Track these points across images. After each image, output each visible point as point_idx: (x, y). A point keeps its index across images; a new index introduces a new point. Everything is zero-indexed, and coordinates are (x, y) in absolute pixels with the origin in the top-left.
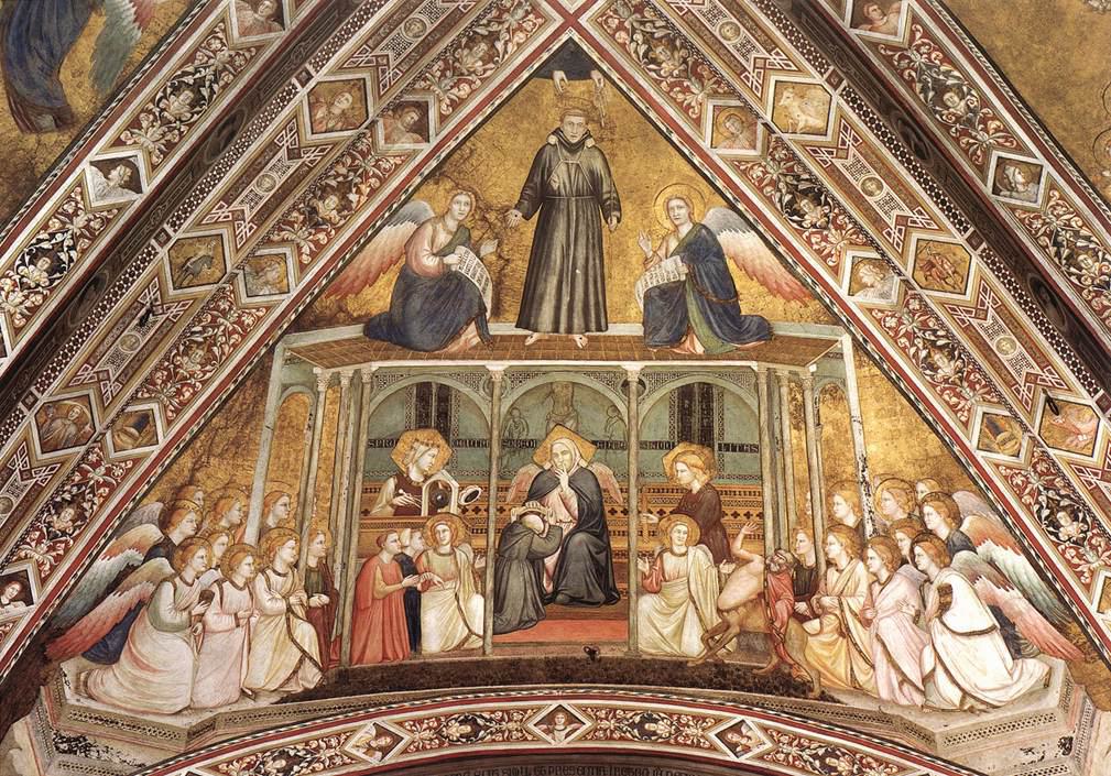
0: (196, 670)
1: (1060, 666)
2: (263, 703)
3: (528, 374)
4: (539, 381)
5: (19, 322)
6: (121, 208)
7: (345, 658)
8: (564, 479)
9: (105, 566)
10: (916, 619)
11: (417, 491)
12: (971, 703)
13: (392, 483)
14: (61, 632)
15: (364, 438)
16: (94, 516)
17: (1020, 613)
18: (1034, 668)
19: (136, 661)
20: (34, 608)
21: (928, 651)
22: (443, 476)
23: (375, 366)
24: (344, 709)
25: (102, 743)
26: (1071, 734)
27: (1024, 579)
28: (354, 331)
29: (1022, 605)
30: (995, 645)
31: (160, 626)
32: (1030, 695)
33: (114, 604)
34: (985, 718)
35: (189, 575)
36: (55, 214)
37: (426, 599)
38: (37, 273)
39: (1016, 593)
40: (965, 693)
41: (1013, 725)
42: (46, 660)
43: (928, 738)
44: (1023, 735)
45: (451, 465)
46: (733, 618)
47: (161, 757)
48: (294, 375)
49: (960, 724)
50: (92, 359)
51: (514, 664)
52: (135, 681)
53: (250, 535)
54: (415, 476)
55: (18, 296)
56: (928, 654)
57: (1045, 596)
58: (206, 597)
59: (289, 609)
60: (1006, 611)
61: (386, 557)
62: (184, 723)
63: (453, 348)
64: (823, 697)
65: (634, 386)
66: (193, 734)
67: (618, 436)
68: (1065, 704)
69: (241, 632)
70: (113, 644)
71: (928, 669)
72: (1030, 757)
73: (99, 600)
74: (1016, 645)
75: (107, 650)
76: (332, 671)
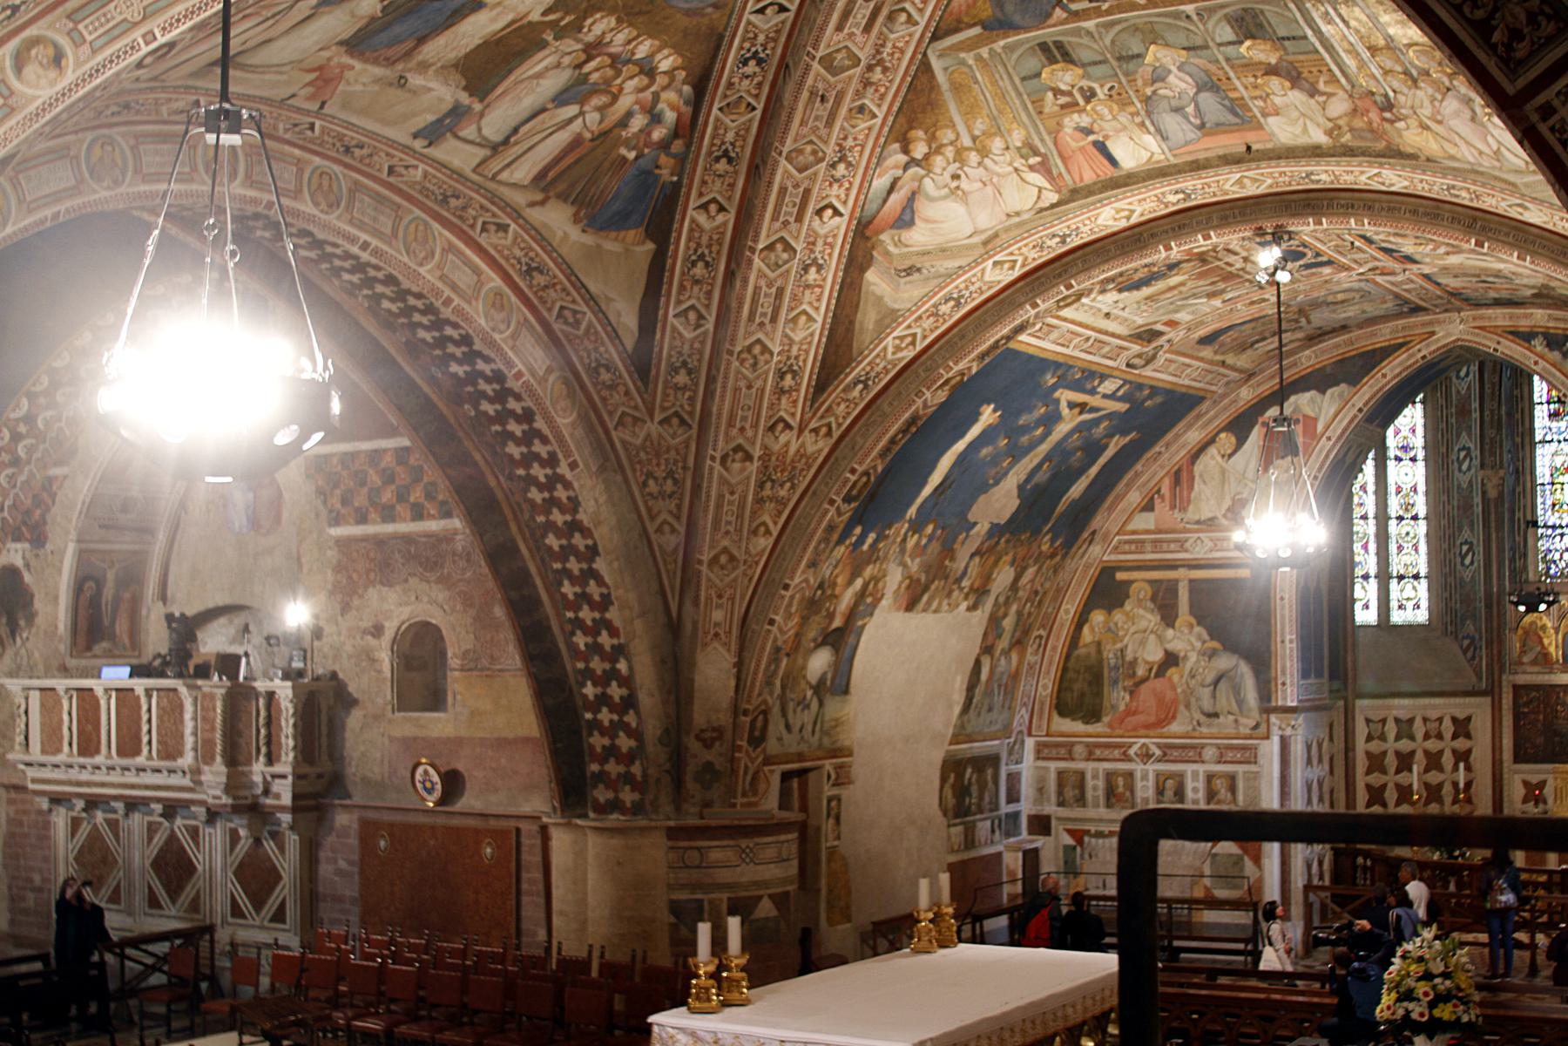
0: (970, 214)
2: (1025, 216)
3: (1113, 24)
4: (1124, 25)
5: (754, 92)
6: (783, 22)
7: (1070, 182)
8: (1174, 69)
9: (880, 183)
10: (1473, 119)
11: (1070, 94)
13: (1050, 95)
14: (870, 222)
15: (1017, 80)
16: (858, 163)
19: (927, 221)
20: (846, 218)
21: (1489, 138)
22: (1085, 83)
23: (1002, 43)
24: (1082, 207)
25: (927, 265)
28: (977, 30)
31: (932, 200)
33: (896, 199)
35: (938, 170)
36: (743, 40)
37: (1109, 144)
38: (752, 67)
42: (868, 239)
43: (1513, 185)
45: (1086, 76)
46: (1341, 122)
47: (971, 259)
48: (948, 61)
50: (803, 123)
51: (1196, 161)
52: (932, 230)
53: (966, 141)
54: (1063, 87)
55: (746, 82)
58: (956, 177)
59: (1016, 170)
61: (1068, 130)
62: (977, 239)
63: (1051, 21)
64: (1428, 160)
65: (1195, 18)
66: (985, 243)
67: (1199, 42)
69: (989, 189)
70: (907, 217)
73: (885, 201)
75: (905, 219)
76: (1064, 191)
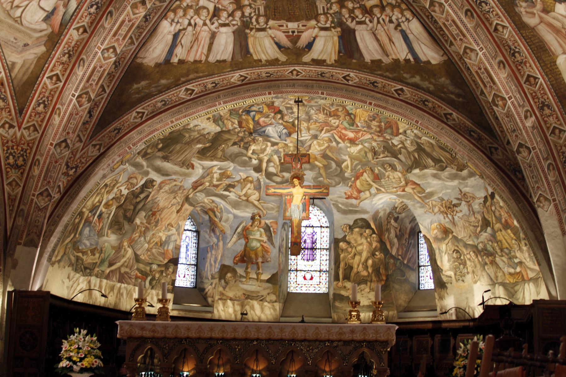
1: (50, 30)
12: (19, 20)
17: (58, 14)
18: (44, 26)
26: (30, 45)
27: (69, 10)
29: (61, 13)
30: (43, 15)
32: (34, 30)
34: (17, 25)
39: (64, 10)
40: (21, 17)
41: (20, 31)
44: (18, 35)
49: (11, 22)
56: (25, 3)
57: (68, 17)
60: (56, 11)
68: (38, 38)
71: (21, 5)
72: (14, 41)
74: (47, 19)
